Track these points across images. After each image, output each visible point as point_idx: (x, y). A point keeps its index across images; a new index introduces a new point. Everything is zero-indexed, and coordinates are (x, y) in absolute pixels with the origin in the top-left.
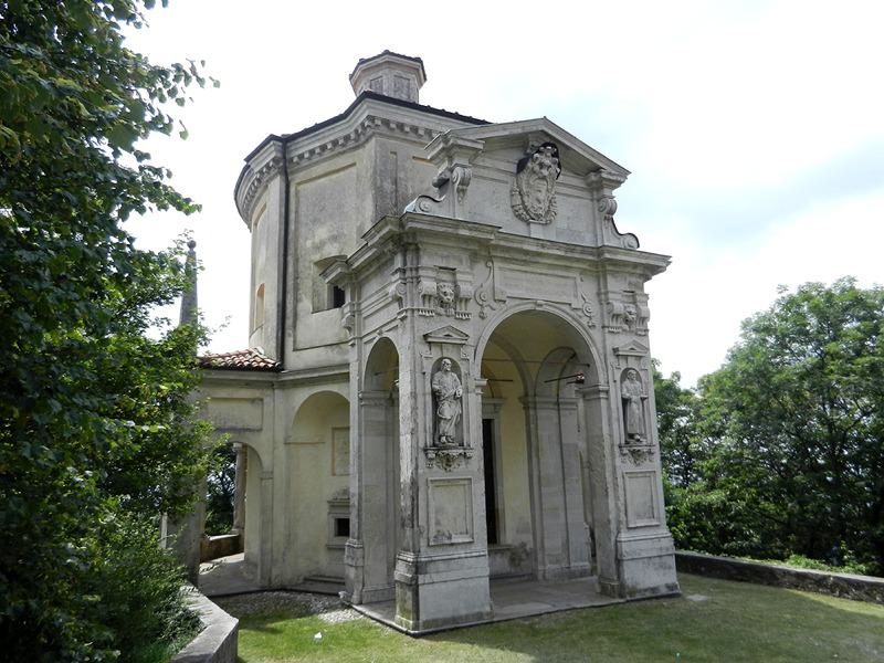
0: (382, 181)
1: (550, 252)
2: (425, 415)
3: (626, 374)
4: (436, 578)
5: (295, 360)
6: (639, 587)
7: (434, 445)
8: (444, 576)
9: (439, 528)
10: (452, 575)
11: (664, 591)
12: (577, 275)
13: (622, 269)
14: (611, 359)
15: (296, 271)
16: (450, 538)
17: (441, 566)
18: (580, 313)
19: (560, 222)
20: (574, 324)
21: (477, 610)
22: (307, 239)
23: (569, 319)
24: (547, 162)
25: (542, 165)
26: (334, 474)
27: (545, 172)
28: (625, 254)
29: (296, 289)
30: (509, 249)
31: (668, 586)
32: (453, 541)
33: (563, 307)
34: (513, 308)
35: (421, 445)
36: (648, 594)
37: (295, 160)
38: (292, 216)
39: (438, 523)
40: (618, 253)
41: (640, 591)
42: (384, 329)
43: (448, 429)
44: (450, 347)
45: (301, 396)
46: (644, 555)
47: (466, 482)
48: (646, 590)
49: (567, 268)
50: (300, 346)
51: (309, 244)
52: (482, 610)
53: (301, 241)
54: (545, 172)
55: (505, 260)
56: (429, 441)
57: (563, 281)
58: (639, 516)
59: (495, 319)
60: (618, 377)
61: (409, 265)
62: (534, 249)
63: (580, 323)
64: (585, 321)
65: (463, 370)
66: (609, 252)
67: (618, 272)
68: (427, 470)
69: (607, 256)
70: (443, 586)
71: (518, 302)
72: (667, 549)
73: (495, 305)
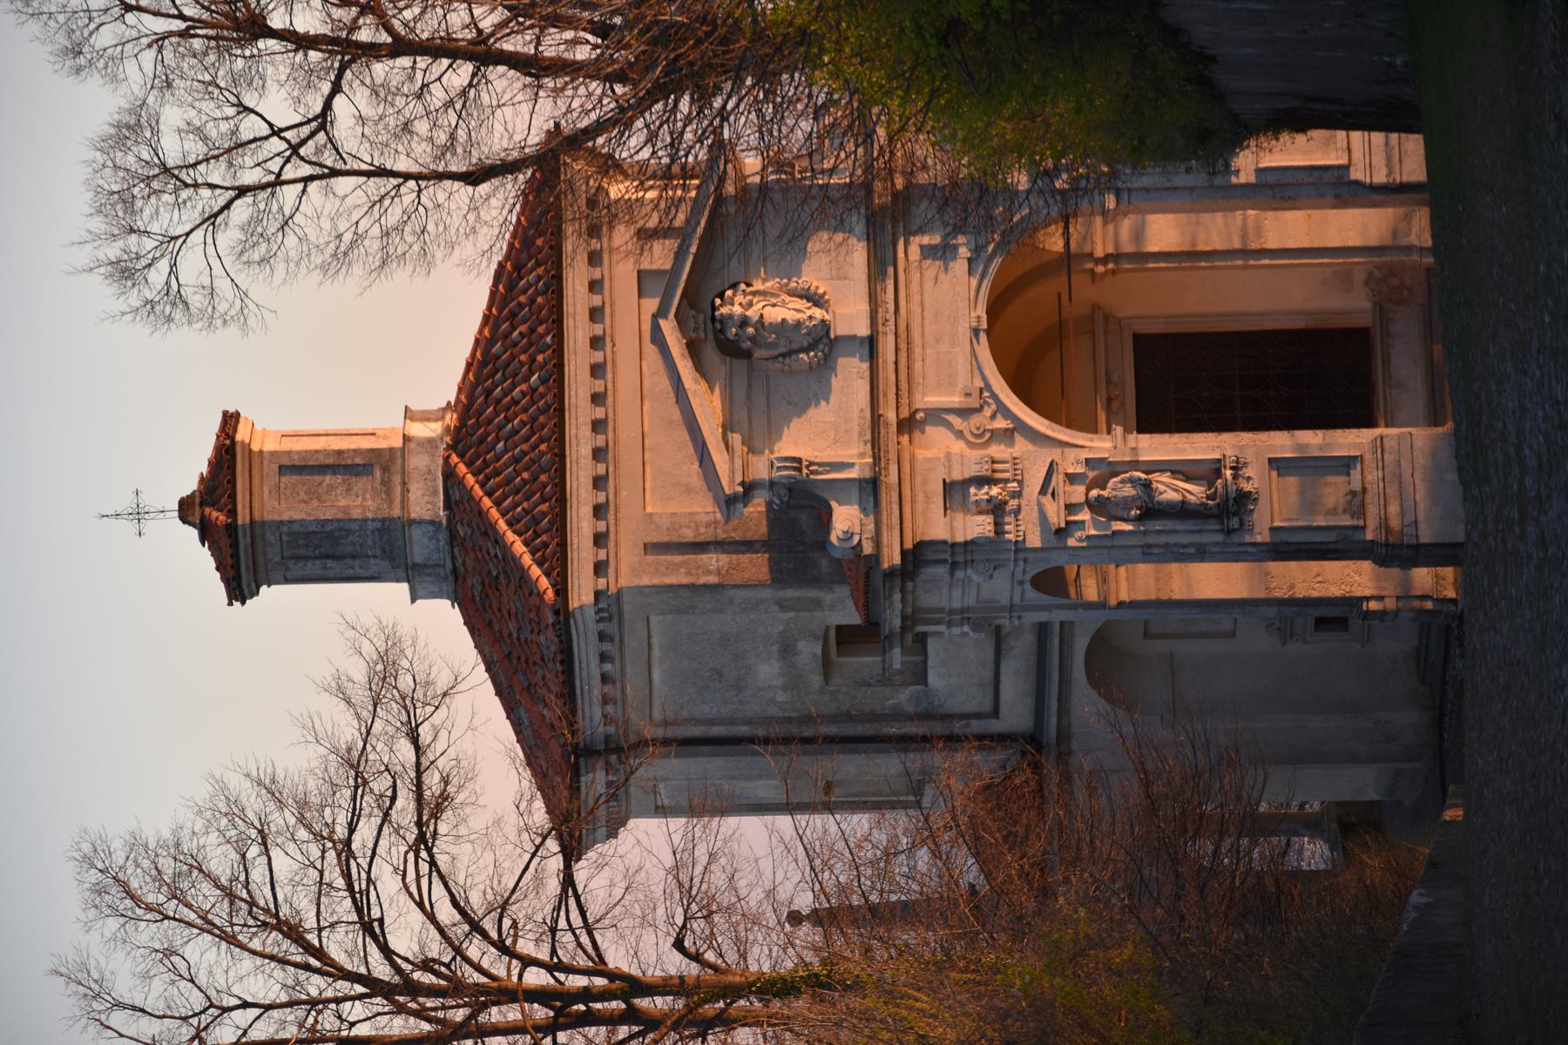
0: (709, 572)
2: (1175, 532)
5: (1016, 714)
7: (1219, 517)
9: (1340, 509)
15: (835, 718)
22: (772, 701)
26: (1233, 634)
29: (874, 717)
35: (1220, 538)
37: (611, 730)
38: (717, 731)
42: (1019, 576)
43: (1195, 492)
45: (1086, 703)
50: (988, 706)
51: (781, 697)
53: (773, 711)
56: (1213, 525)
61: (947, 556)
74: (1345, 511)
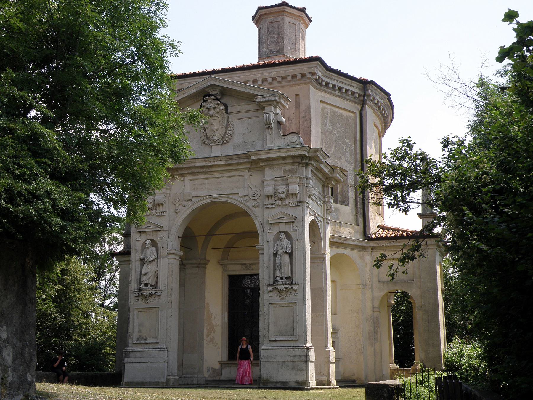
1: (216, 163)
3: (277, 238)
4: (134, 360)
6: (272, 380)
8: (138, 360)
9: (140, 334)
10: (143, 360)
11: (293, 385)
12: (245, 173)
13: (274, 162)
14: (267, 227)
16: (145, 340)
17: (138, 354)
18: (247, 198)
19: (237, 139)
20: (242, 206)
21: (156, 380)
23: (238, 204)
24: (211, 106)
25: (209, 109)
27: (212, 112)
28: (267, 153)
30: (190, 168)
31: (297, 382)
32: (147, 342)
33: (230, 196)
34: (198, 203)
36: (278, 385)
39: (140, 331)
40: (259, 155)
41: (272, 382)
44: (151, 233)
46: (278, 359)
47: (157, 309)
48: (277, 382)
49: (236, 170)
52: (160, 381)
54: (212, 112)
55: (191, 174)
57: (236, 178)
58: (281, 334)
59: (186, 211)
60: (271, 237)
62: (203, 164)
63: (247, 205)
64: (250, 204)
65: (160, 246)
66: (253, 155)
67: (273, 165)
68: (135, 303)
69: (253, 157)
70: (138, 365)
71: (201, 198)
72: (300, 356)
73: (185, 203)
74: (140, 336)
